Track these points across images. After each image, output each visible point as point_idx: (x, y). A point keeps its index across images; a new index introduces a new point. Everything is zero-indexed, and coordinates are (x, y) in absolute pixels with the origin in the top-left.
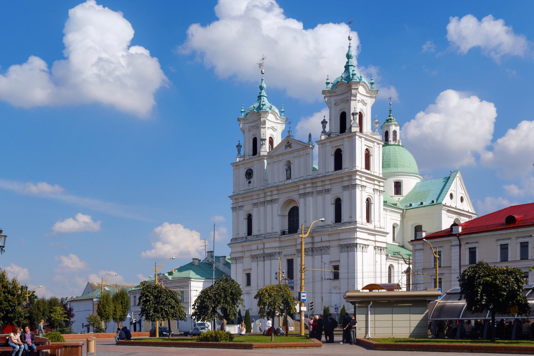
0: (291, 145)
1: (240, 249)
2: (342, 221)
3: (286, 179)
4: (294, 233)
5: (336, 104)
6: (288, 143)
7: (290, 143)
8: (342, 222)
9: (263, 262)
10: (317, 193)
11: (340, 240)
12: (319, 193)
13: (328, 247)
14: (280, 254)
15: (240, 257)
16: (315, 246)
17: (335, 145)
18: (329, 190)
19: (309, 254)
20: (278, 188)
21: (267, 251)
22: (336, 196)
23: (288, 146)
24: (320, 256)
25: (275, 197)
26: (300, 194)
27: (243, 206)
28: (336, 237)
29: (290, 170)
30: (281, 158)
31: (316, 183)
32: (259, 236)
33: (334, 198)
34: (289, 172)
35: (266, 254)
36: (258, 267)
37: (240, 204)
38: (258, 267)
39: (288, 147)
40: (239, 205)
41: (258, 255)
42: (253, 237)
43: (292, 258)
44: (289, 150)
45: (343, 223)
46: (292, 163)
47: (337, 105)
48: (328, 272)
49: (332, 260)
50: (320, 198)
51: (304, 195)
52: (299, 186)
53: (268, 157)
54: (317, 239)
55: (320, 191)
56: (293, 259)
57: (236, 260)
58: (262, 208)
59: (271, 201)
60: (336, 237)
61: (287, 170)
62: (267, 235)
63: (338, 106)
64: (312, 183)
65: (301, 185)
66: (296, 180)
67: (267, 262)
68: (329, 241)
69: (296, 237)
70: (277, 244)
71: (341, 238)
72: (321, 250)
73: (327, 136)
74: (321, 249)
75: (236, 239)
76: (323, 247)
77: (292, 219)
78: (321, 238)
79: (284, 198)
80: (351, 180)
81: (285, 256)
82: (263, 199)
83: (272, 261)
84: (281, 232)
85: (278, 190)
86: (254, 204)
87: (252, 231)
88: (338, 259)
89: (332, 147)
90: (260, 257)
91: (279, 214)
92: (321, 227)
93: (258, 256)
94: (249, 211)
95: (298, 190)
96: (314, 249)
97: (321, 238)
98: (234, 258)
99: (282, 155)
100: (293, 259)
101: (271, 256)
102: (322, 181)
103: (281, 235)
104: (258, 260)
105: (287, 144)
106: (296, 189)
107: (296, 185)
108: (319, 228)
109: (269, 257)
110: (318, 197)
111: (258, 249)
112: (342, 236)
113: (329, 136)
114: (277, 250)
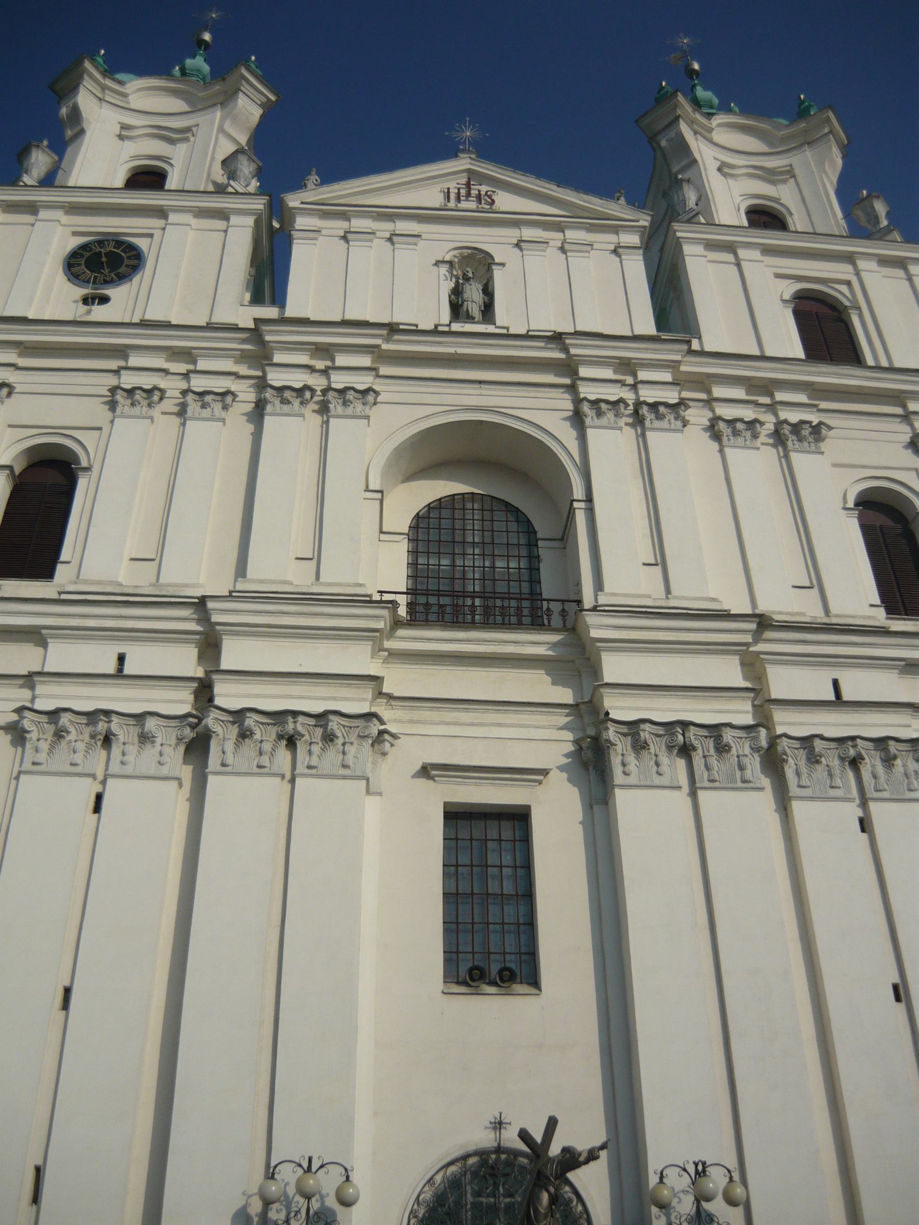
5: (726, 170)
10: (717, 436)
12: (736, 433)
18: (824, 431)
46: (503, 265)
47: (725, 175)
53: (302, 203)
63: (731, 181)
77: (445, 561)
78: (836, 683)
87: (63, 557)
91: (371, 487)
102: (753, 385)
104: (115, 768)
109: (267, 747)
111: (127, 671)
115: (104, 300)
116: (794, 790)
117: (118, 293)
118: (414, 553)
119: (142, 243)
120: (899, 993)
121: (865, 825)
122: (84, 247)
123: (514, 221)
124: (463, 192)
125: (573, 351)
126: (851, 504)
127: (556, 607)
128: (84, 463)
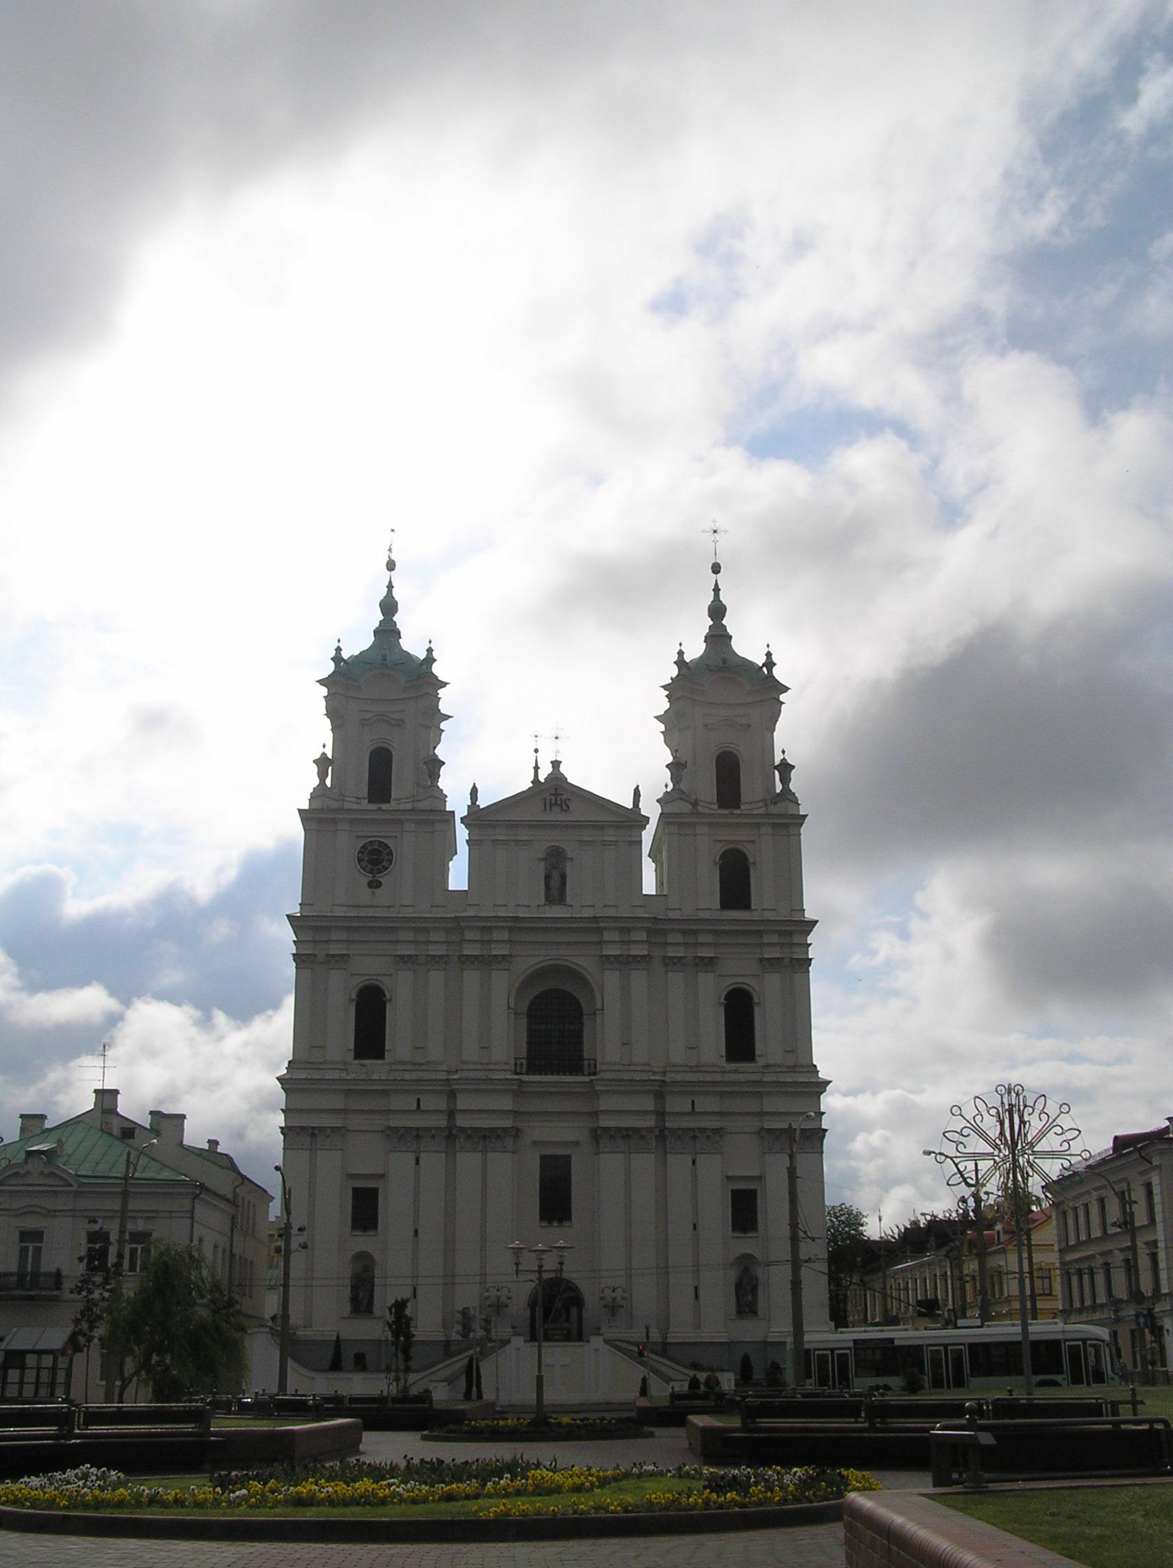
0: (567, 802)
1: (338, 1102)
2: (757, 1058)
3: (543, 901)
4: (565, 1075)
6: (556, 794)
7: (564, 797)
8: (761, 1061)
9: (443, 1155)
10: (666, 965)
11: (762, 1114)
12: (674, 964)
13: (718, 1131)
14: (519, 1134)
15: (335, 1130)
16: (667, 1125)
17: (728, 838)
19: (650, 1147)
20: (515, 925)
21: (461, 1121)
22: (736, 983)
23: (556, 804)
24: (689, 1158)
25: (497, 950)
26: (608, 957)
27: (348, 955)
28: (753, 1106)
29: (563, 877)
30: (524, 835)
31: (664, 932)
32: (424, 1067)
33: (729, 986)
34: (555, 882)
35: (462, 1130)
36: (417, 1174)
37: (335, 950)
38: (417, 1174)
39: (556, 809)
40: (332, 952)
41: (428, 1129)
42: (394, 1067)
43: (569, 1153)
44: (556, 816)
45: (767, 1066)
48: (717, 1212)
49: (730, 1174)
50: (676, 980)
51: (627, 962)
52: (600, 931)
54: (676, 1104)
55: (680, 958)
56: (569, 1157)
57: (313, 1135)
58: (436, 978)
59: (486, 962)
60: (751, 1105)
61: (548, 878)
62: (466, 1067)
64: (650, 931)
65: (611, 929)
66: (586, 913)
67: (468, 1161)
68: (722, 1114)
69: (597, 1088)
70: (506, 1103)
71: (765, 1110)
72: (694, 1137)
73: (690, 807)
74: (694, 1135)
75: (310, 1063)
76: (704, 1130)
78: (693, 1101)
79: (539, 959)
80: (791, 945)
81: (535, 1143)
82: (444, 947)
83: (489, 1154)
84: (516, 1064)
85: (511, 929)
86: (402, 957)
87: (387, 1048)
88: (755, 1173)
89: (714, 841)
90: (433, 1137)
92: (688, 1069)
93: (420, 1133)
94: (379, 978)
95: (600, 942)
96: (666, 1132)
97: (693, 1101)
98: (302, 1128)
99: (530, 826)
100: (569, 1157)
101: (485, 1138)
103: (516, 1073)
105: (553, 798)
106: (596, 938)
107: (595, 926)
108: (679, 1069)
110: (670, 975)
111: (423, 1107)
112: (770, 1104)
113: (693, 808)
114: (507, 1123)
115: (379, 885)
116: (668, 1150)
117: (384, 879)
118: (530, 1024)
119: (390, 843)
120: (695, 1227)
121: (694, 1162)
122: (364, 847)
123: (579, 826)
124: (553, 802)
125: (601, 925)
126: (722, 1000)
127: (586, 1062)
128: (388, 997)
